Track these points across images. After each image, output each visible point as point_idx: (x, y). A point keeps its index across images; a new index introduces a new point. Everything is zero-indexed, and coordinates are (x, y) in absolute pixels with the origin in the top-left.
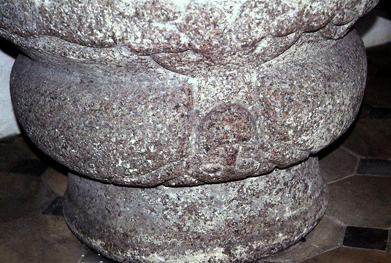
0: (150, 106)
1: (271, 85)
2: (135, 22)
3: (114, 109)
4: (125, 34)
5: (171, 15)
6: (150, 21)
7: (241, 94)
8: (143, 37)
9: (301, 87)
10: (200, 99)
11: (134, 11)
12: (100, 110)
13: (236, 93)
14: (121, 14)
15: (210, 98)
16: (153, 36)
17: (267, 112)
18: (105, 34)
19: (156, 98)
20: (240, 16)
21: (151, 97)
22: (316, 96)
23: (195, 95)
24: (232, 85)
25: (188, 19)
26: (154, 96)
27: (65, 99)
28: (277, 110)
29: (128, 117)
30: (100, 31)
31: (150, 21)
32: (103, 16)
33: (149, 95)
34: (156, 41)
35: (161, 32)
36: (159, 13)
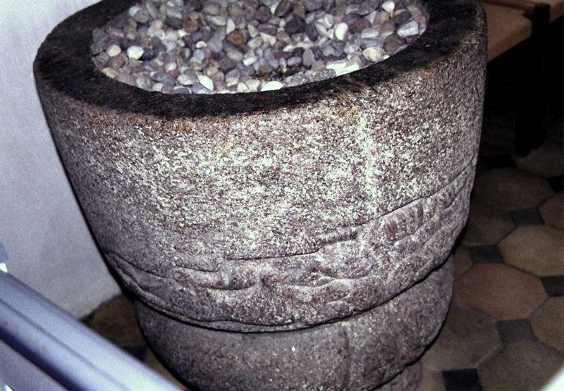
0: (317, 356)
1: (406, 309)
2: (312, 305)
3: (284, 363)
4: (303, 315)
5: (342, 294)
6: (325, 302)
7: (384, 323)
8: (318, 314)
9: (426, 302)
10: (353, 337)
11: (311, 297)
12: (271, 366)
13: (380, 324)
14: (300, 301)
15: (362, 335)
16: (326, 312)
17: (405, 331)
18: (285, 317)
19: (321, 348)
20: (394, 279)
21: (315, 347)
22: (436, 304)
23: (349, 335)
24: (376, 319)
25: (355, 294)
26: (318, 346)
27: (233, 358)
28: (414, 328)
29: (299, 368)
30: (281, 316)
31: (325, 302)
32: (284, 306)
33: (313, 346)
34: (329, 315)
35: (333, 307)
36: (332, 295)
